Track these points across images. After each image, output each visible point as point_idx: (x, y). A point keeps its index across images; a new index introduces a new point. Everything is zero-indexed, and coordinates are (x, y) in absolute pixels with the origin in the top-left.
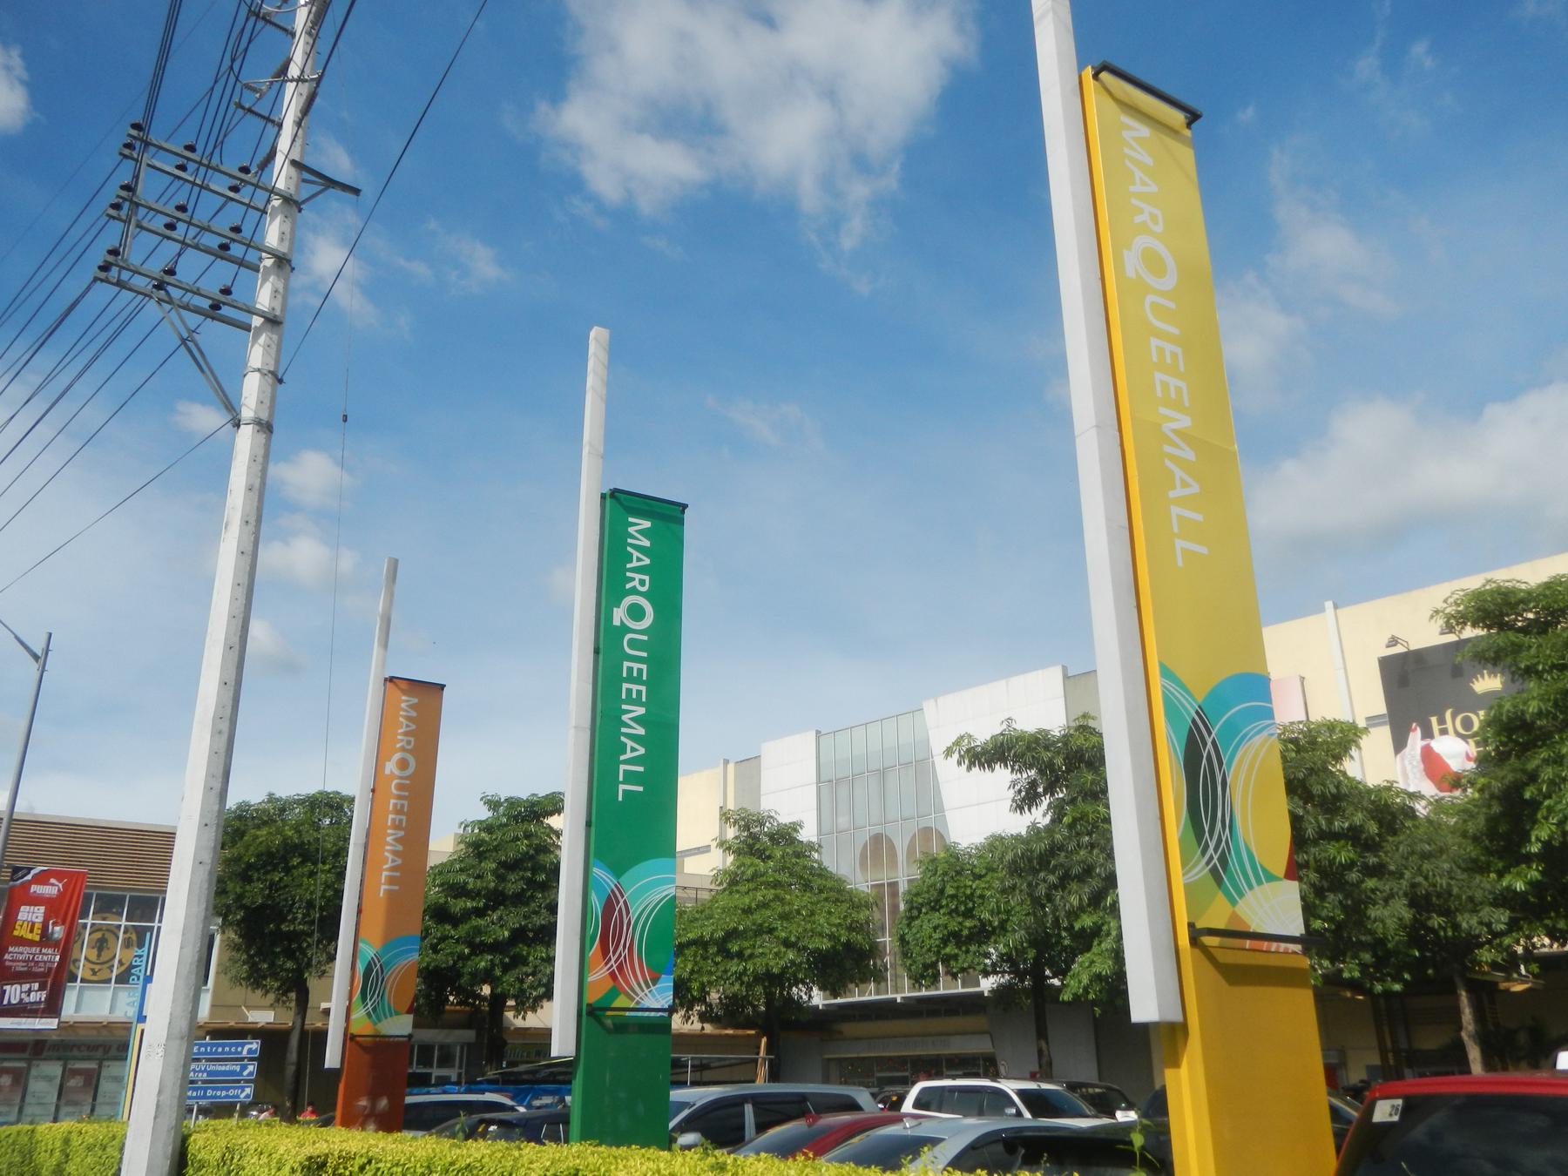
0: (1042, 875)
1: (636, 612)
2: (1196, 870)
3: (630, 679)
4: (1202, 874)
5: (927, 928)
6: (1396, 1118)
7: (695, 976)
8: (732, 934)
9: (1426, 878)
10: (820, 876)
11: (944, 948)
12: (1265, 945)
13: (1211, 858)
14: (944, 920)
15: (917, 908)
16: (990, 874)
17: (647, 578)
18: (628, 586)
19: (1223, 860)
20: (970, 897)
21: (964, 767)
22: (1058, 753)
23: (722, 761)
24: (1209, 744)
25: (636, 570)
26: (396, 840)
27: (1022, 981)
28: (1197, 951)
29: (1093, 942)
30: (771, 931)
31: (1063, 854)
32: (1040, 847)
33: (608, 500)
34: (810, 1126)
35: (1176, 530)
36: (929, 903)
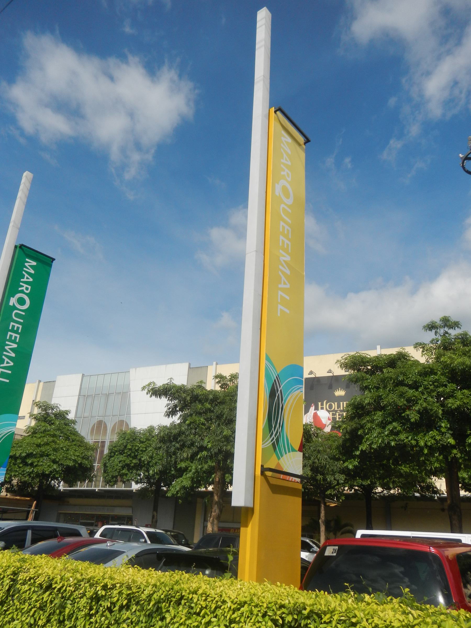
0: (174, 443)
1: (21, 301)
2: (267, 443)
3: (12, 331)
4: (270, 444)
5: (117, 461)
6: (335, 554)
8: (30, 455)
9: (318, 460)
10: (74, 434)
11: (122, 470)
12: (288, 478)
13: (273, 439)
14: (124, 458)
15: (114, 452)
16: (147, 441)
17: (30, 287)
18: (20, 289)
19: (278, 440)
20: (137, 451)
21: (149, 395)
22: (188, 395)
23: (38, 381)
24: (279, 391)
25: (26, 283)
27: (151, 487)
28: (263, 477)
29: (183, 473)
30: (47, 455)
31: (184, 436)
32: (175, 432)
33: (18, 249)
34: (59, 542)
35: (279, 301)
36: (119, 451)
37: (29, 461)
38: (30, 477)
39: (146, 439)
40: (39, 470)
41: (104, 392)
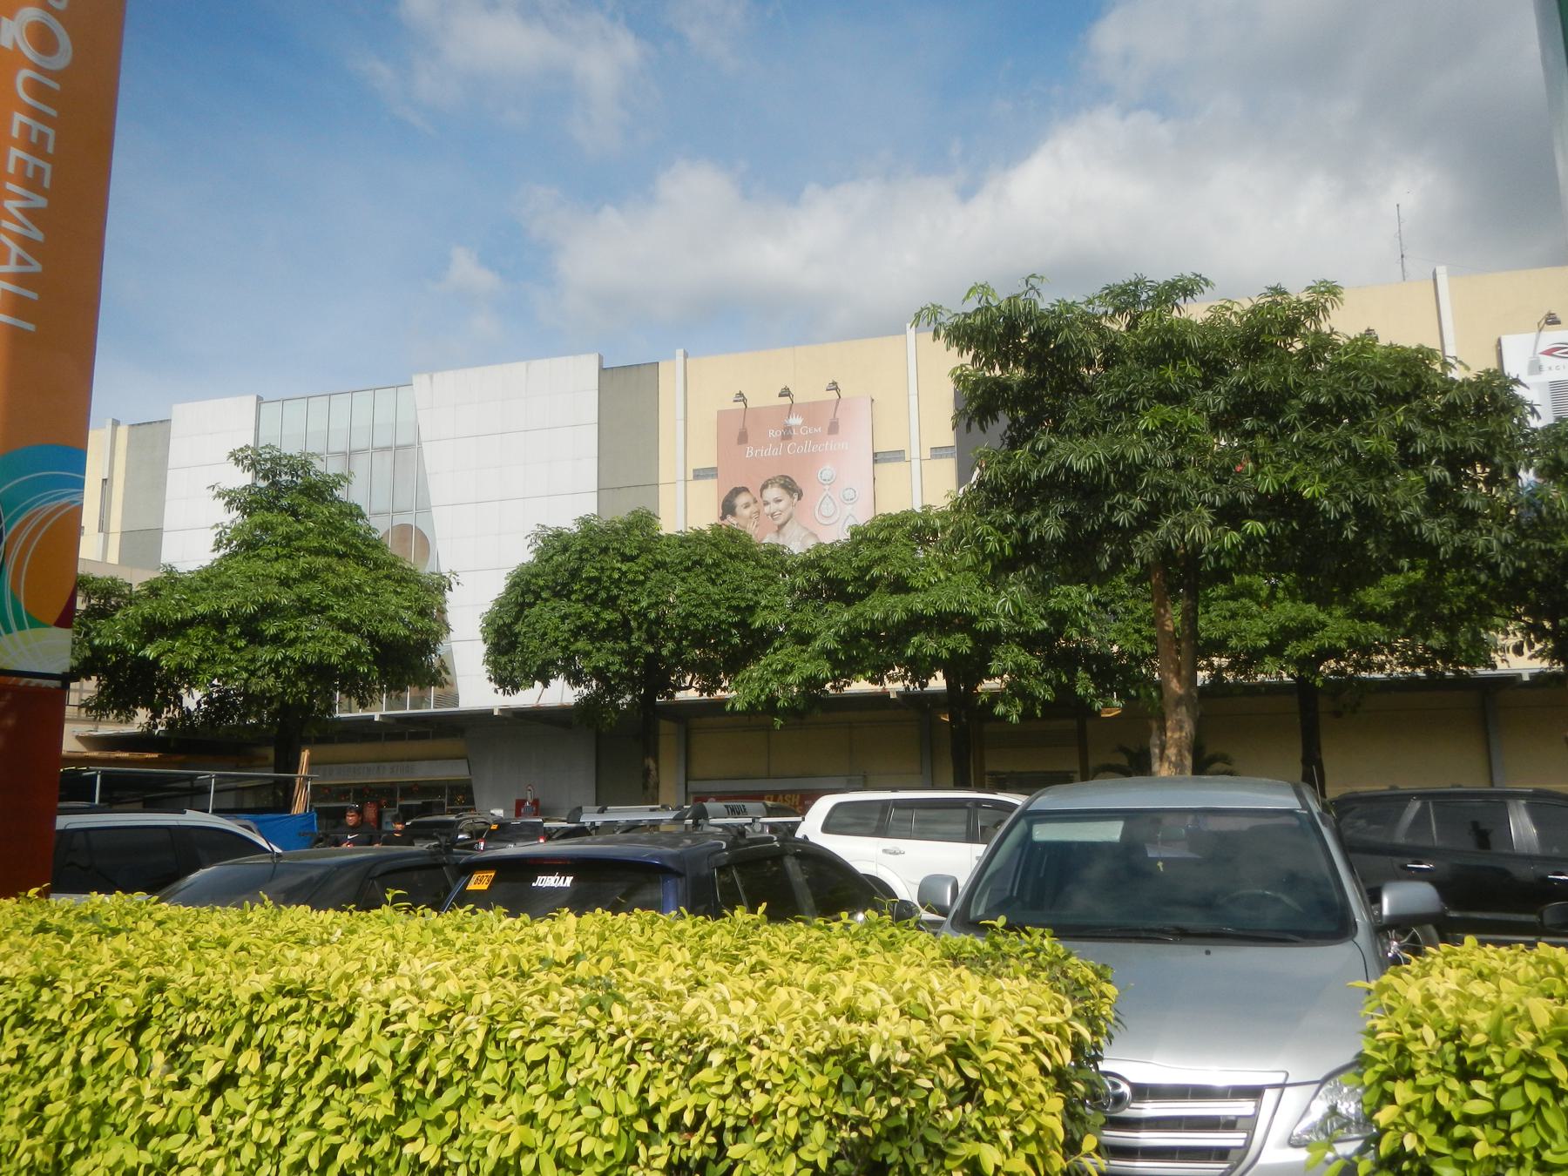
0: (1119, 496)
7: (204, 666)
8: (269, 610)
11: (573, 643)
15: (534, 592)
20: (617, 583)
23: (110, 421)
26: (28, 213)
30: (323, 609)
37: (271, 629)
38: (278, 676)
39: (640, 548)
40: (307, 652)
41: (334, 448)
